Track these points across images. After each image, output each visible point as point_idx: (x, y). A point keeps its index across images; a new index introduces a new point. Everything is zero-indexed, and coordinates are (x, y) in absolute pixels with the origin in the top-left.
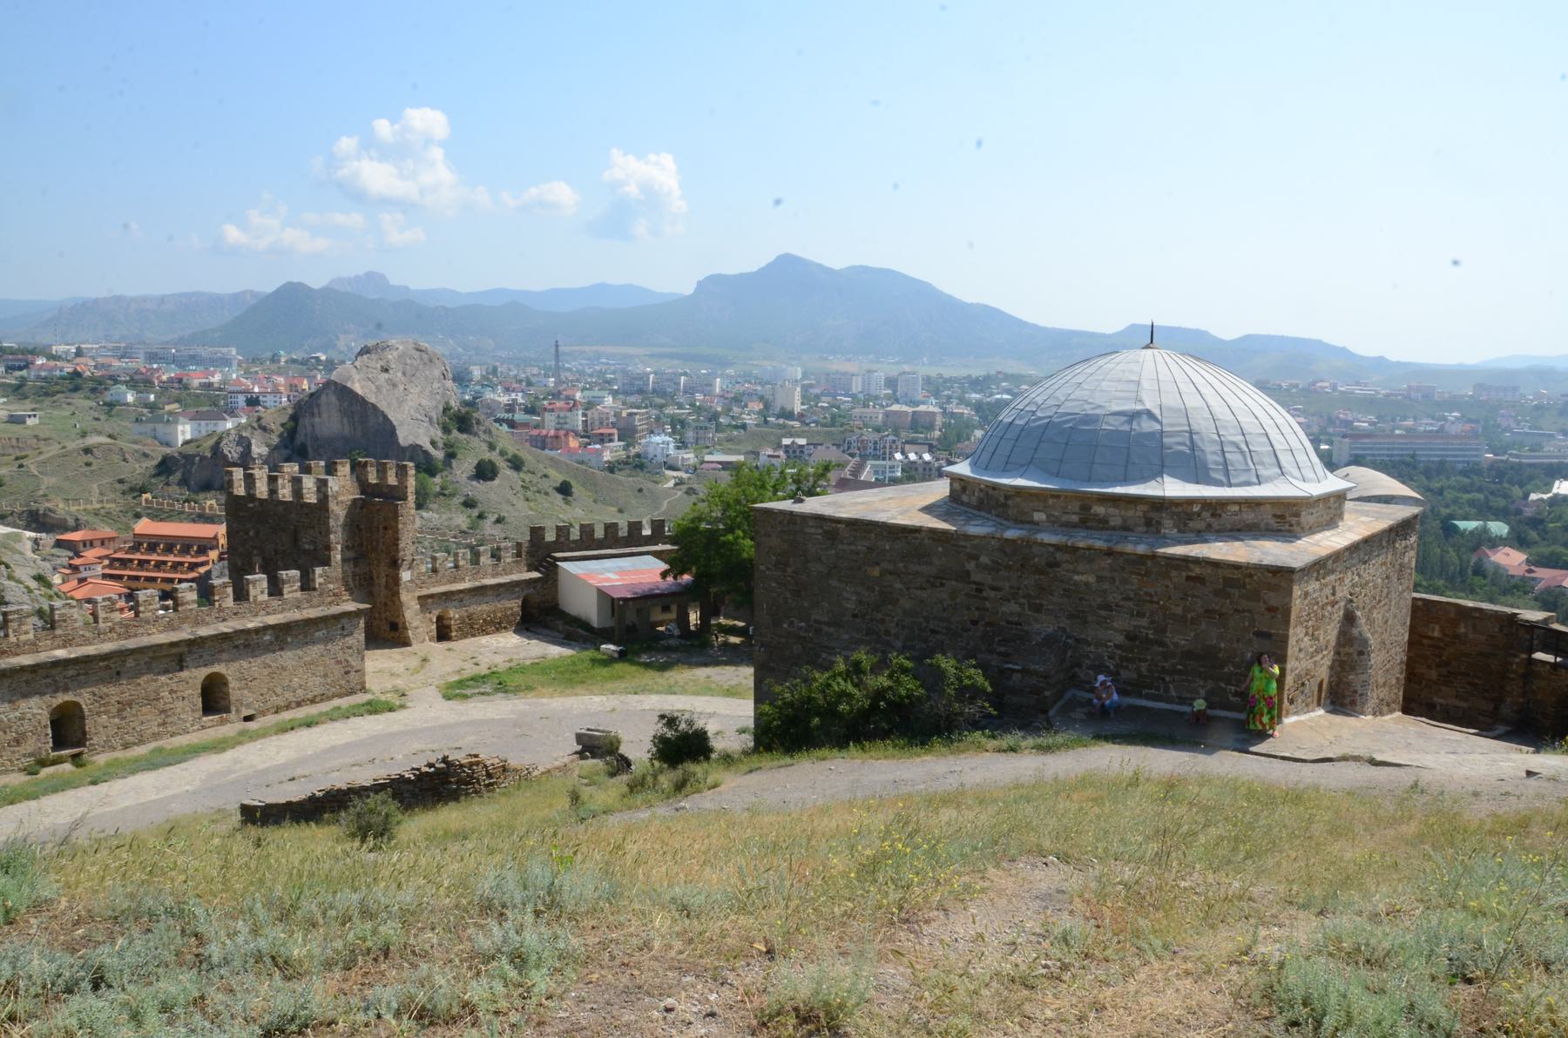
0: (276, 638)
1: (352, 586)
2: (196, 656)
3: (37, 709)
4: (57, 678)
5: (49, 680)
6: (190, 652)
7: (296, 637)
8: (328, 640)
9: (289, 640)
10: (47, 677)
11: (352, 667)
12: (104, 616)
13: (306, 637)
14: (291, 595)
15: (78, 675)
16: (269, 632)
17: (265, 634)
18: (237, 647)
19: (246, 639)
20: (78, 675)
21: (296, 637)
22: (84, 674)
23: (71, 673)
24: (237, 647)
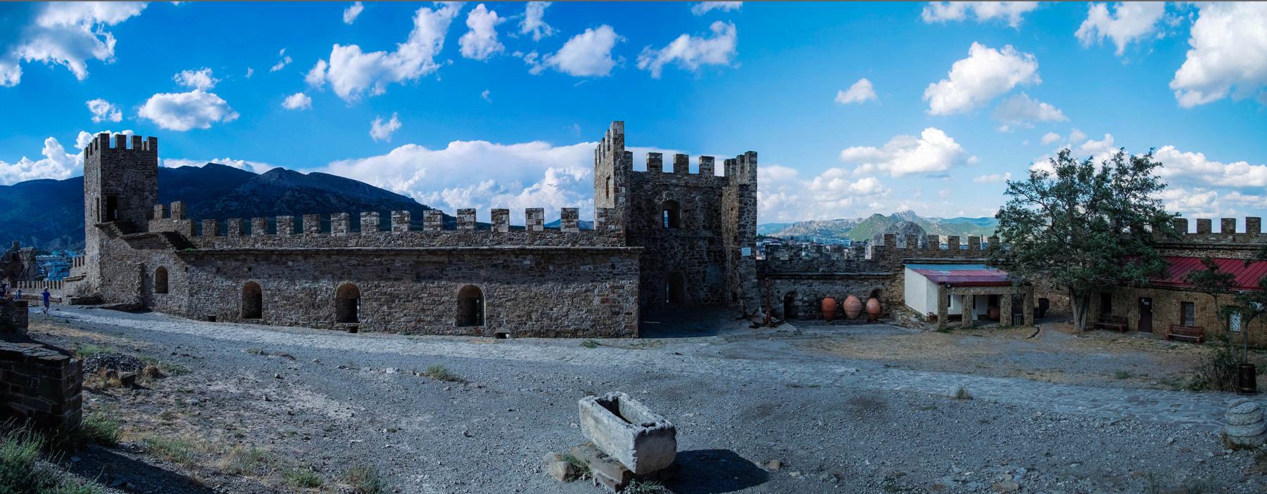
0: (538, 264)
1: (707, 259)
2: (454, 267)
3: (328, 287)
4: (344, 264)
5: (338, 265)
6: (450, 262)
7: (560, 267)
8: (595, 278)
9: (551, 268)
10: (337, 262)
11: (622, 308)
12: (395, 226)
13: (570, 268)
14: (568, 230)
15: (359, 265)
16: (530, 257)
17: (525, 259)
18: (495, 266)
19: (506, 261)
20: (359, 265)
21: (560, 267)
22: (363, 265)
23: (354, 262)
24: (495, 266)
